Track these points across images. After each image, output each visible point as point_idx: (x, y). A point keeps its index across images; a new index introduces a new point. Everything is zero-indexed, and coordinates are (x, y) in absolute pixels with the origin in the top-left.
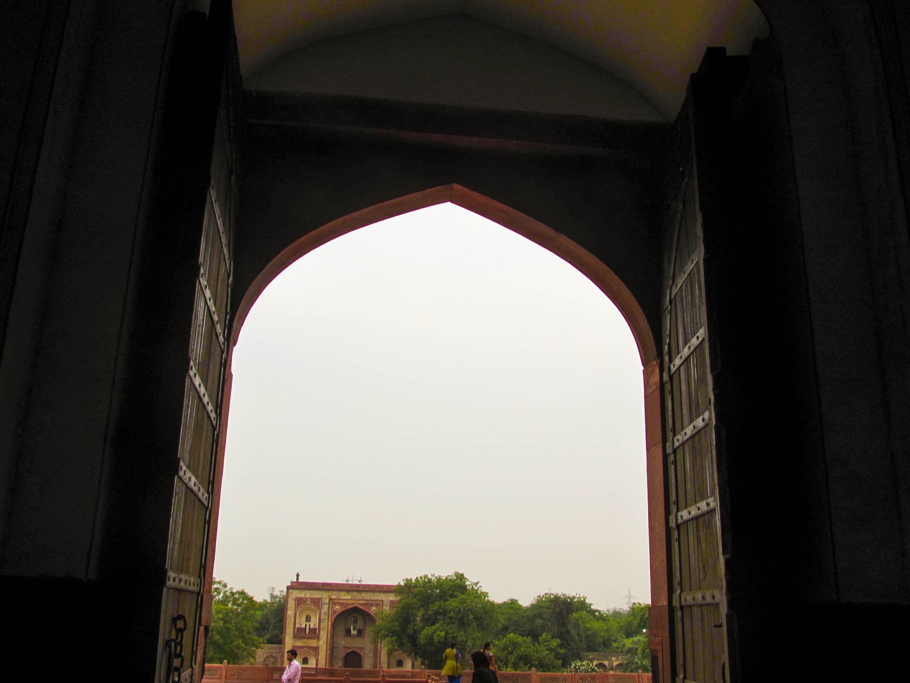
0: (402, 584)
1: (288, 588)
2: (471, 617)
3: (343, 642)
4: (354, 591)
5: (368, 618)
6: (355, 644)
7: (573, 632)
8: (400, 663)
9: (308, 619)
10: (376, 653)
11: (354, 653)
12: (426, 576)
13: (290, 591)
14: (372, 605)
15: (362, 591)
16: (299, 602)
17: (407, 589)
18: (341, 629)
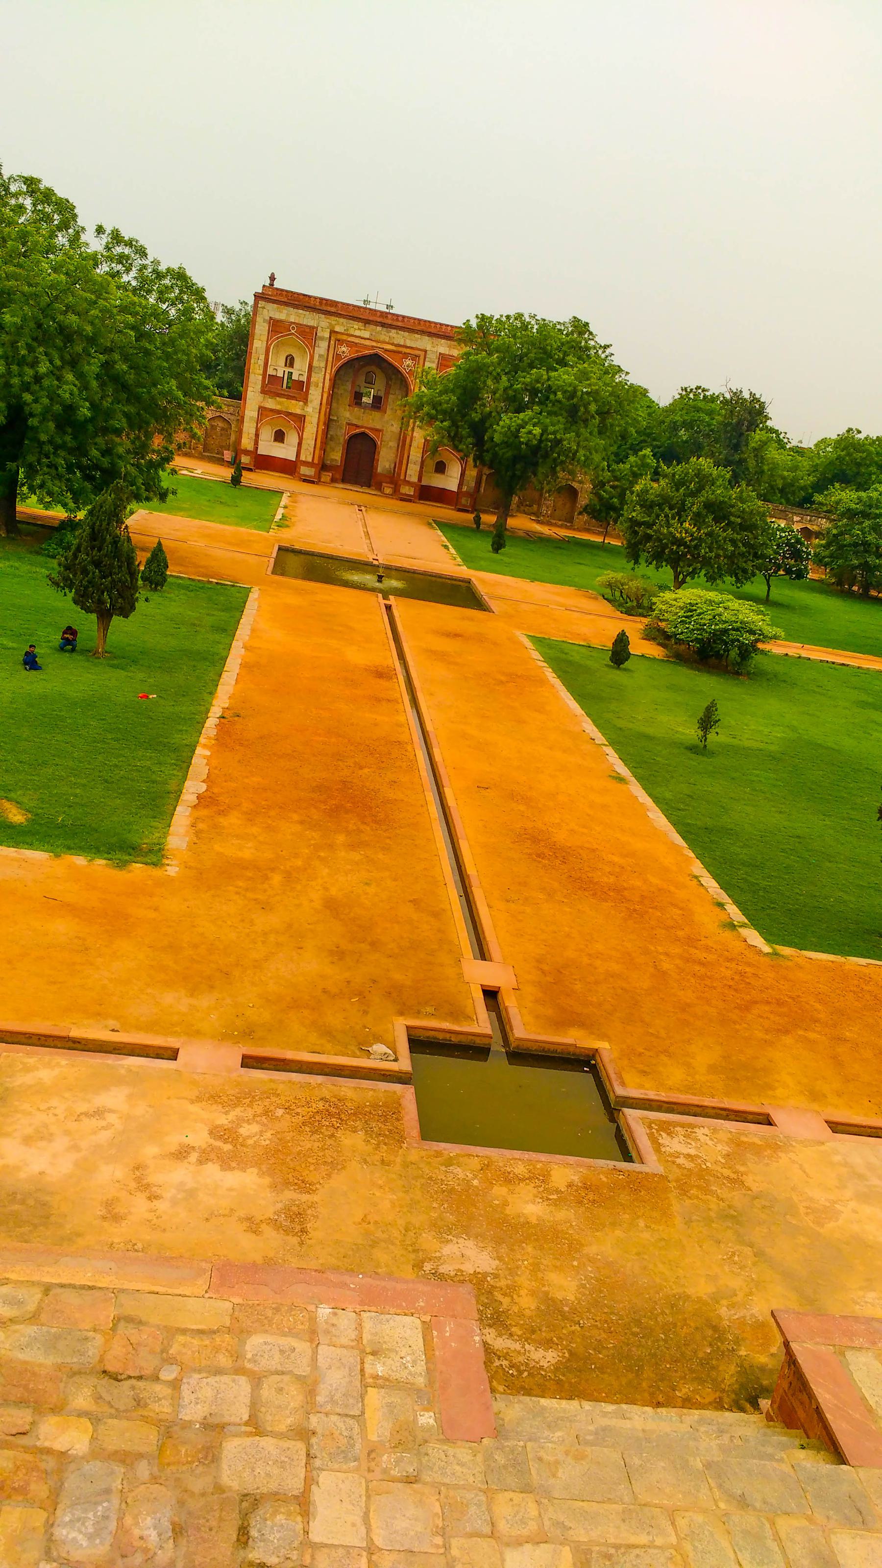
0: (474, 323)
1: (258, 297)
2: (593, 408)
3: (347, 414)
4: (377, 323)
5: (396, 378)
6: (369, 420)
7: (751, 463)
8: (441, 468)
9: (290, 361)
10: (403, 443)
11: (363, 433)
12: (519, 316)
13: (261, 303)
14: (406, 356)
15: (391, 326)
16: (276, 326)
17: (481, 333)
18: (346, 390)
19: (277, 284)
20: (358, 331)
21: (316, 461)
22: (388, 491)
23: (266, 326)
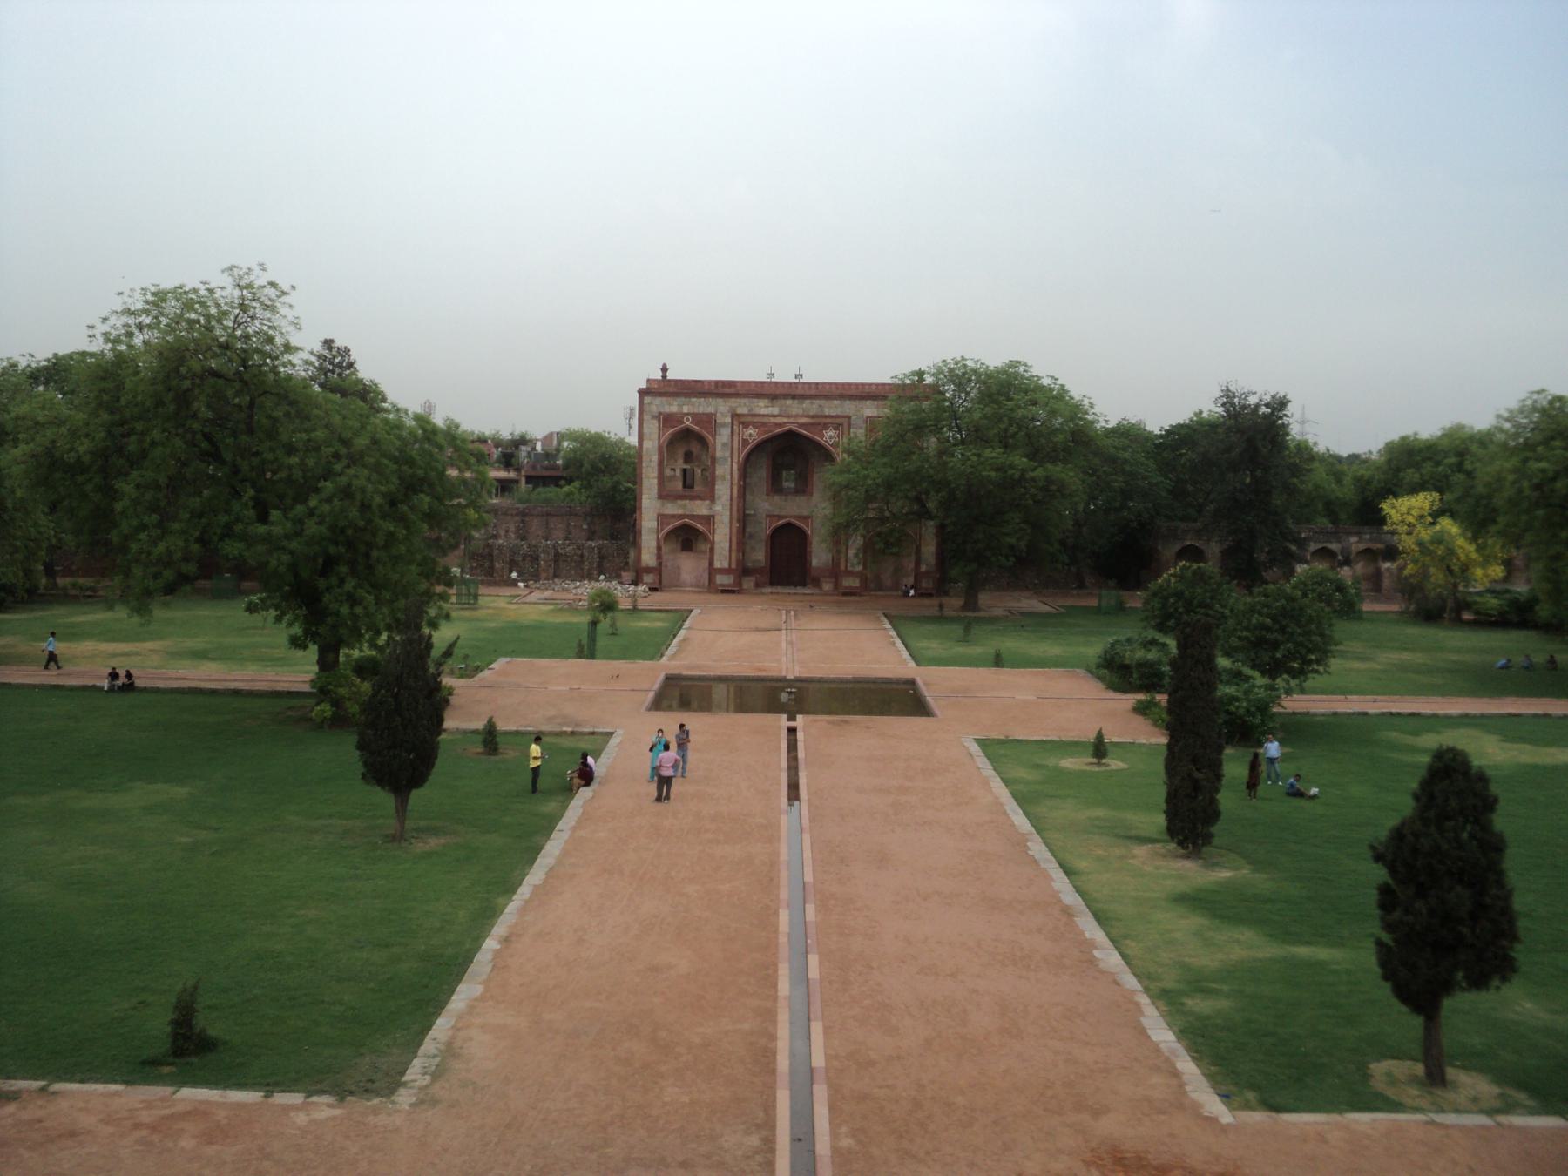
4: (786, 396)
6: (791, 508)
11: (789, 525)
13: (647, 400)
15: (803, 397)
19: (670, 376)
20: (763, 407)
21: (734, 566)
22: (827, 586)
23: (655, 422)
